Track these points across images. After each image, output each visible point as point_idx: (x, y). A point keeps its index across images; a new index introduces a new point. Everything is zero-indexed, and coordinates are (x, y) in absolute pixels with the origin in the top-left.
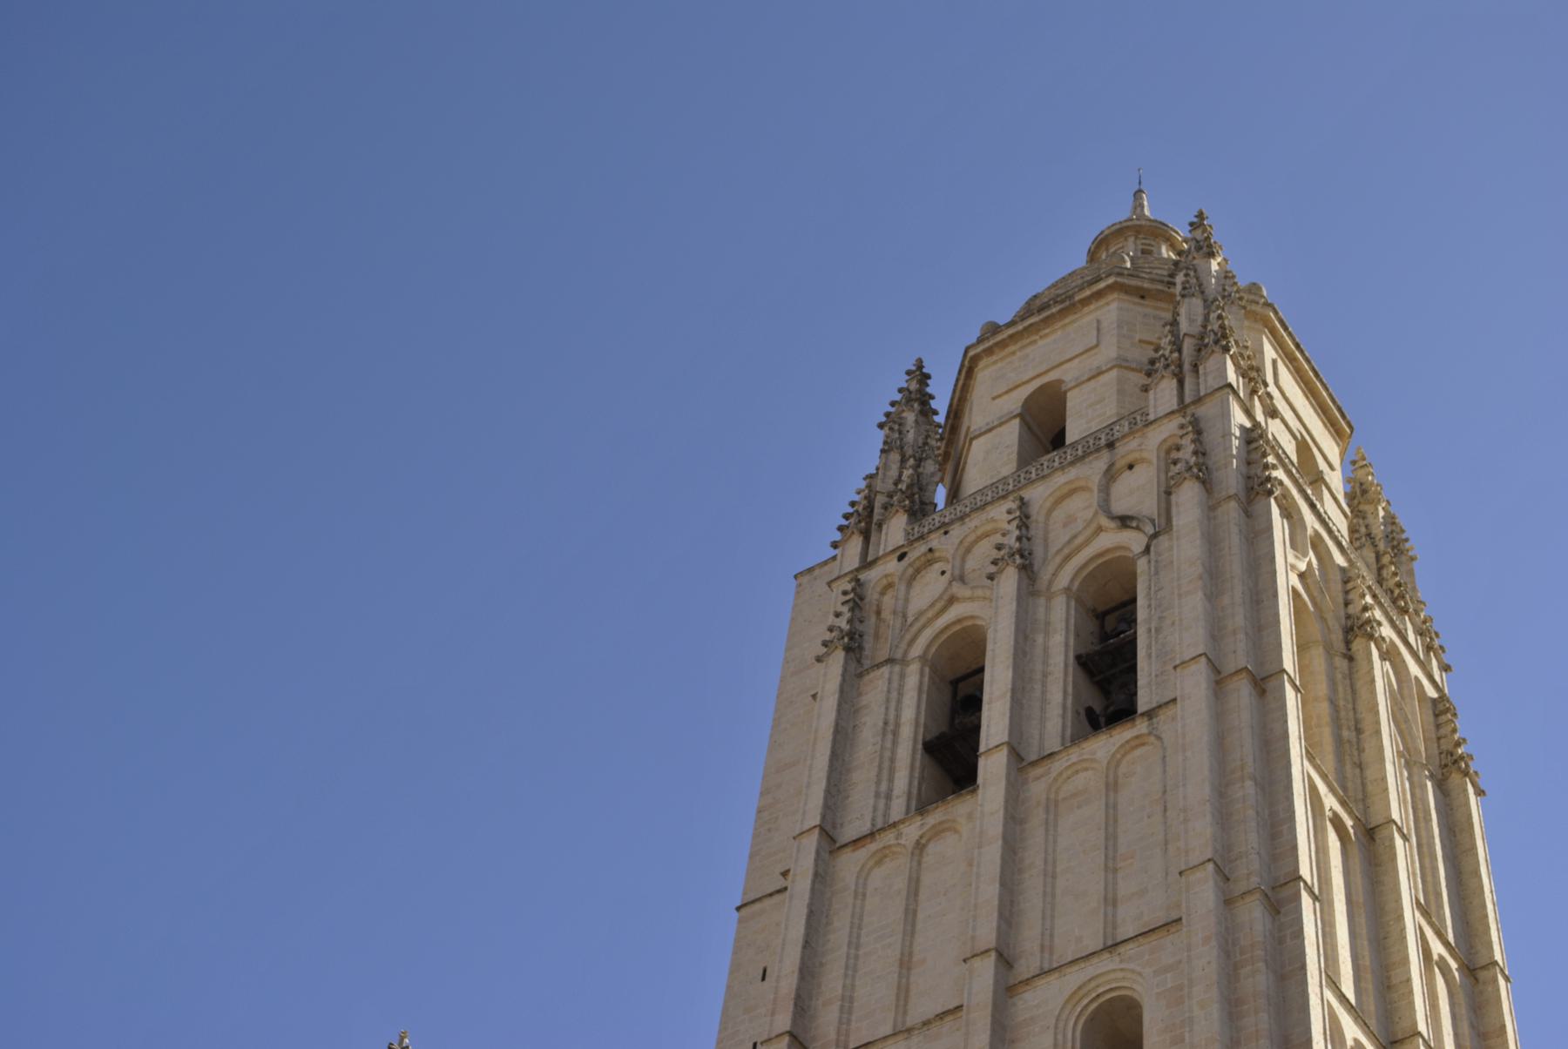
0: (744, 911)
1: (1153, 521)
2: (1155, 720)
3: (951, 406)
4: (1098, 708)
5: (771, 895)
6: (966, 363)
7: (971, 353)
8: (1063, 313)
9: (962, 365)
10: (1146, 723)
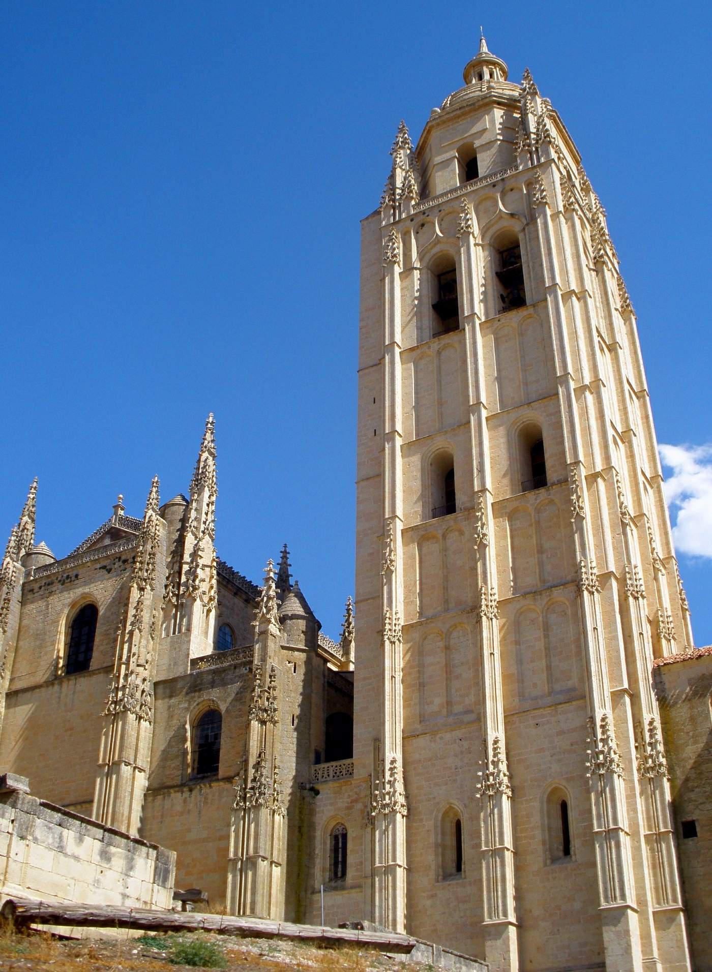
0: (361, 373)
1: (525, 217)
3: (419, 144)
4: (505, 295)
6: (428, 128)
7: (430, 124)
8: (470, 111)
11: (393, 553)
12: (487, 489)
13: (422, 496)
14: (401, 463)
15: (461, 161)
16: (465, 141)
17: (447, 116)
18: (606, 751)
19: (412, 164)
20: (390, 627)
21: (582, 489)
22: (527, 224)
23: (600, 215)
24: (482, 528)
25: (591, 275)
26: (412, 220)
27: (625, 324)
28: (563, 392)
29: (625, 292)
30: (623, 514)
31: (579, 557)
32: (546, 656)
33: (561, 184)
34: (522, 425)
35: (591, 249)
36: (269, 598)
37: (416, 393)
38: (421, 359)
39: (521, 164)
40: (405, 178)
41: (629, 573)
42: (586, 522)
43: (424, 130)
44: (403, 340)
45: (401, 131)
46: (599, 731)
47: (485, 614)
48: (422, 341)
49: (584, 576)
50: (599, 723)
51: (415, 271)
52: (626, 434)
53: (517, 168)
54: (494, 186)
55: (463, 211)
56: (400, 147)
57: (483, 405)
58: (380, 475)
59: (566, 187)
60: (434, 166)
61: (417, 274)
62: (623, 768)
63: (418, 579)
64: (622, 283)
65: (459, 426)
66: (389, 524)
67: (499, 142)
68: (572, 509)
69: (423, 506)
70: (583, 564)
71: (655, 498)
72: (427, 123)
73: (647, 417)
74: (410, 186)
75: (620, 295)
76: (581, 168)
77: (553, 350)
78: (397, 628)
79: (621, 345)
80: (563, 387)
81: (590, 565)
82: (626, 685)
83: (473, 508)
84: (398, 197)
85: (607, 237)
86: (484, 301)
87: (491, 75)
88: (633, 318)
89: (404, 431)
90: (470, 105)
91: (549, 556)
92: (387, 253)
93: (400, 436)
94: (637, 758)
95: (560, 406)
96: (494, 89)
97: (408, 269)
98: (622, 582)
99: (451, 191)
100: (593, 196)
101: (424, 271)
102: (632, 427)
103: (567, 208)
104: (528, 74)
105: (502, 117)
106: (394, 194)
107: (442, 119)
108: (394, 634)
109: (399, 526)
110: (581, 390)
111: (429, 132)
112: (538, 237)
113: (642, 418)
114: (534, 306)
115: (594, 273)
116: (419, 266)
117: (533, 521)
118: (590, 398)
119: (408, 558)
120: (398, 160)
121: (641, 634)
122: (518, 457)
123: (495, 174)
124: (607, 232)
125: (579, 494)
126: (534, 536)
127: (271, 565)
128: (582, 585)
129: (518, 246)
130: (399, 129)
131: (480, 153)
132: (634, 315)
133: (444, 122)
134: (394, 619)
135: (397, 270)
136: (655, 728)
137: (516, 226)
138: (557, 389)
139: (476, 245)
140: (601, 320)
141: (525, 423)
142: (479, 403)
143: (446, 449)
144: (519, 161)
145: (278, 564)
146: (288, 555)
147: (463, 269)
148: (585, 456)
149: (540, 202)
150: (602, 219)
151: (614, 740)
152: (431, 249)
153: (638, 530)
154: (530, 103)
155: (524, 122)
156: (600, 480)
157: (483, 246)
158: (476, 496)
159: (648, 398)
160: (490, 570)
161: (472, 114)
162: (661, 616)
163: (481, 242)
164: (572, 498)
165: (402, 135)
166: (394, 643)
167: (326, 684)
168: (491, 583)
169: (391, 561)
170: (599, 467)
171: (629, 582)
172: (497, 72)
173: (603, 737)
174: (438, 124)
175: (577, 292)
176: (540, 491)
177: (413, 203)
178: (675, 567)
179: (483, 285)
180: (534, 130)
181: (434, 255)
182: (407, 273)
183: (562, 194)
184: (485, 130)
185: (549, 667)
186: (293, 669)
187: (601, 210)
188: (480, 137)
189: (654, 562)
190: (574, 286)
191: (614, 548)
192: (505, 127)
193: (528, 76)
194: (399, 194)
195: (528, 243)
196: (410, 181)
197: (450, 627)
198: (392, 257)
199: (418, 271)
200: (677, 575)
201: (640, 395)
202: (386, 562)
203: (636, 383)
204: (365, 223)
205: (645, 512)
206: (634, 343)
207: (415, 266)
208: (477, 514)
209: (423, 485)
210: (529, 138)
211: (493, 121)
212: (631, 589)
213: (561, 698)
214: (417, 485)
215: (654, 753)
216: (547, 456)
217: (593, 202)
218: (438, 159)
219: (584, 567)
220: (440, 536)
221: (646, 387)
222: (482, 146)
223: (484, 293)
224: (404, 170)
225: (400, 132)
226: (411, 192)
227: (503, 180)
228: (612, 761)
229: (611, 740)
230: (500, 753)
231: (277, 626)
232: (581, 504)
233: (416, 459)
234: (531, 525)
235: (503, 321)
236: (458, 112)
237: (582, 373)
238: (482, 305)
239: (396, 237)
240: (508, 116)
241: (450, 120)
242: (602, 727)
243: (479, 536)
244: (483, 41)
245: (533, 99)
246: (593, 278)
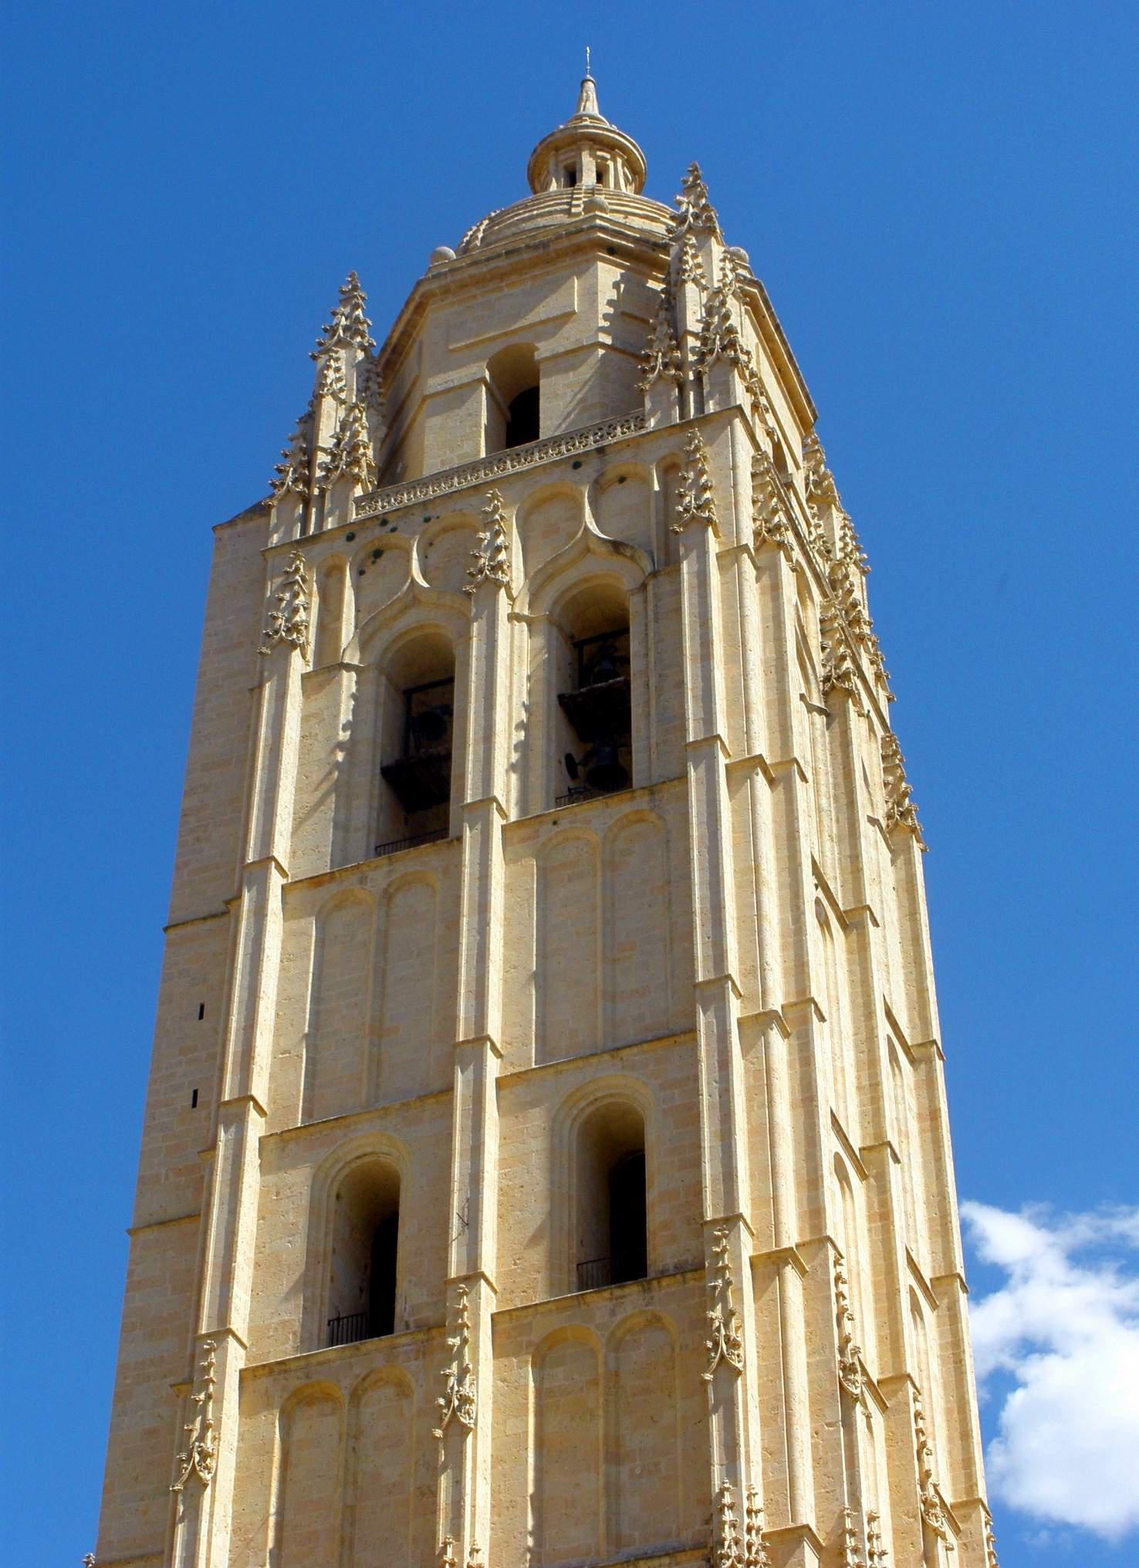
0: (172, 933)
1: (651, 553)
2: (657, 796)
3: (390, 338)
5: (205, 919)
6: (417, 297)
7: (422, 289)
8: (533, 264)
10: (647, 798)
11: (210, 1434)
12: (483, 1276)
13: (305, 1283)
14: (257, 1187)
15: (496, 392)
16: (515, 340)
17: (473, 271)
19: (367, 389)
21: (740, 1290)
22: (654, 574)
23: (852, 569)
24: (460, 1382)
25: (813, 724)
26: (351, 538)
27: (893, 862)
28: (708, 1025)
29: (901, 779)
30: (848, 1369)
33: (754, 475)
34: (591, 1109)
35: (818, 656)
37: (316, 999)
38: (338, 907)
39: (653, 413)
40: (344, 426)
41: (853, 1534)
42: (745, 1385)
43: (407, 304)
44: (294, 853)
45: (347, 298)
48: (345, 860)
49: (728, 1533)
51: (345, 674)
52: (874, 1154)
53: (641, 421)
54: (577, 465)
55: (489, 523)
56: (340, 343)
57: (493, 1044)
58: (198, 1216)
59: (767, 484)
60: (424, 399)
61: (348, 682)
63: (273, 1510)
64: (895, 753)
65: (421, 1098)
66: (208, 1351)
67: (601, 352)
68: (710, 1344)
69: (305, 1308)
70: (727, 1499)
71: (941, 1335)
72: (419, 283)
73: (934, 1115)
74: (355, 447)
75: (886, 784)
76: (815, 442)
77: (690, 912)
79: (879, 919)
80: (711, 1013)
81: (746, 1504)
83: (442, 1325)
84: (319, 473)
85: (866, 630)
86: (521, 767)
87: (601, 177)
88: (917, 848)
89: (273, 1100)
90: (536, 247)
91: (638, 1471)
92: (275, 618)
93: (261, 1111)
95: (696, 1062)
96: (603, 209)
97: (327, 668)
99: (461, 471)
100: (837, 518)
101: (371, 675)
102: (892, 1136)
103: (764, 541)
104: (697, 178)
105: (616, 285)
106: (309, 464)
107: (458, 276)
109: (236, 1359)
110: (760, 1023)
111: (420, 308)
112: (678, 610)
113: (920, 1117)
114: (651, 790)
115: (820, 720)
116: (356, 662)
117: (601, 1370)
118: (780, 1047)
119: (251, 1451)
120: (331, 375)
122: (574, 1193)
123: (583, 435)
124: (865, 614)
125: (731, 1306)
126: (601, 1413)
128: (722, 1557)
129: (627, 630)
130: (343, 293)
131: (549, 375)
132: (918, 841)
133: (463, 286)
135: (299, 665)
137: (622, 576)
138: (693, 1016)
139: (513, 617)
140: (828, 845)
141: (599, 1104)
142: (481, 1038)
143: (382, 1159)
144: (648, 405)
147: (473, 677)
148: (756, 1202)
149: (693, 517)
150: (856, 578)
152: (395, 618)
153: (886, 1420)
154: (694, 256)
155: (672, 303)
156: (790, 1273)
157: (530, 622)
158: (450, 1294)
159: (939, 1064)
160: (474, 1499)
161: (537, 272)
163: (526, 612)
165: (347, 310)
168: (473, 1536)
169: (205, 1455)
170: (792, 1234)
172: (617, 169)
174: (446, 291)
175: (768, 762)
176: (627, 1291)
177: (358, 491)
178: (986, 1532)
179: (521, 726)
180: (697, 328)
181: (401, 635)
182: (321, 678)
183: (754, 502)
184: (568, 316)
187: (857, 555)
188: (553, 334)
189: (927, 1512)
190: (762, 746)
191: (817, 1461)
192: (623, 314)
193: (694, 185)
195: (651, 625)
196: (355, 434)
198: (289, 631)
199: (354, 674)
201: (919, 1055)
202: (190, 1457)
203: (911, 1020)
204: (226, 533)
205: (911, 1368)
206: (913, 914)
207: (346, 660)
208: (451, 1341)
209: (311, 1253)
210: (680, 345)
211: (590, 294)
214: (295, 1250)
216: (652, 1195)
217: (838, 533)
218: (435, 383)
219: (731, 1507)
220: (344, 1394)
221: (936, 1034)
222: (555, 357)
223: (523, 747)
224: (343, 402)
225: (344, 302)
226: (356, 462)
227: (601, 451)
232: (733, 1334)
233: (299, 1179)
234: (595, 1382)
235: (564, 824)
236: (502, 263)
237: (763, 978)
238: (514, 777)
239: (304, 580)
240: (632, 284)
241: (479, 281)
243: (449, 1402)
244: (590, 86)
245: (702, 246)
246: (818, 733)
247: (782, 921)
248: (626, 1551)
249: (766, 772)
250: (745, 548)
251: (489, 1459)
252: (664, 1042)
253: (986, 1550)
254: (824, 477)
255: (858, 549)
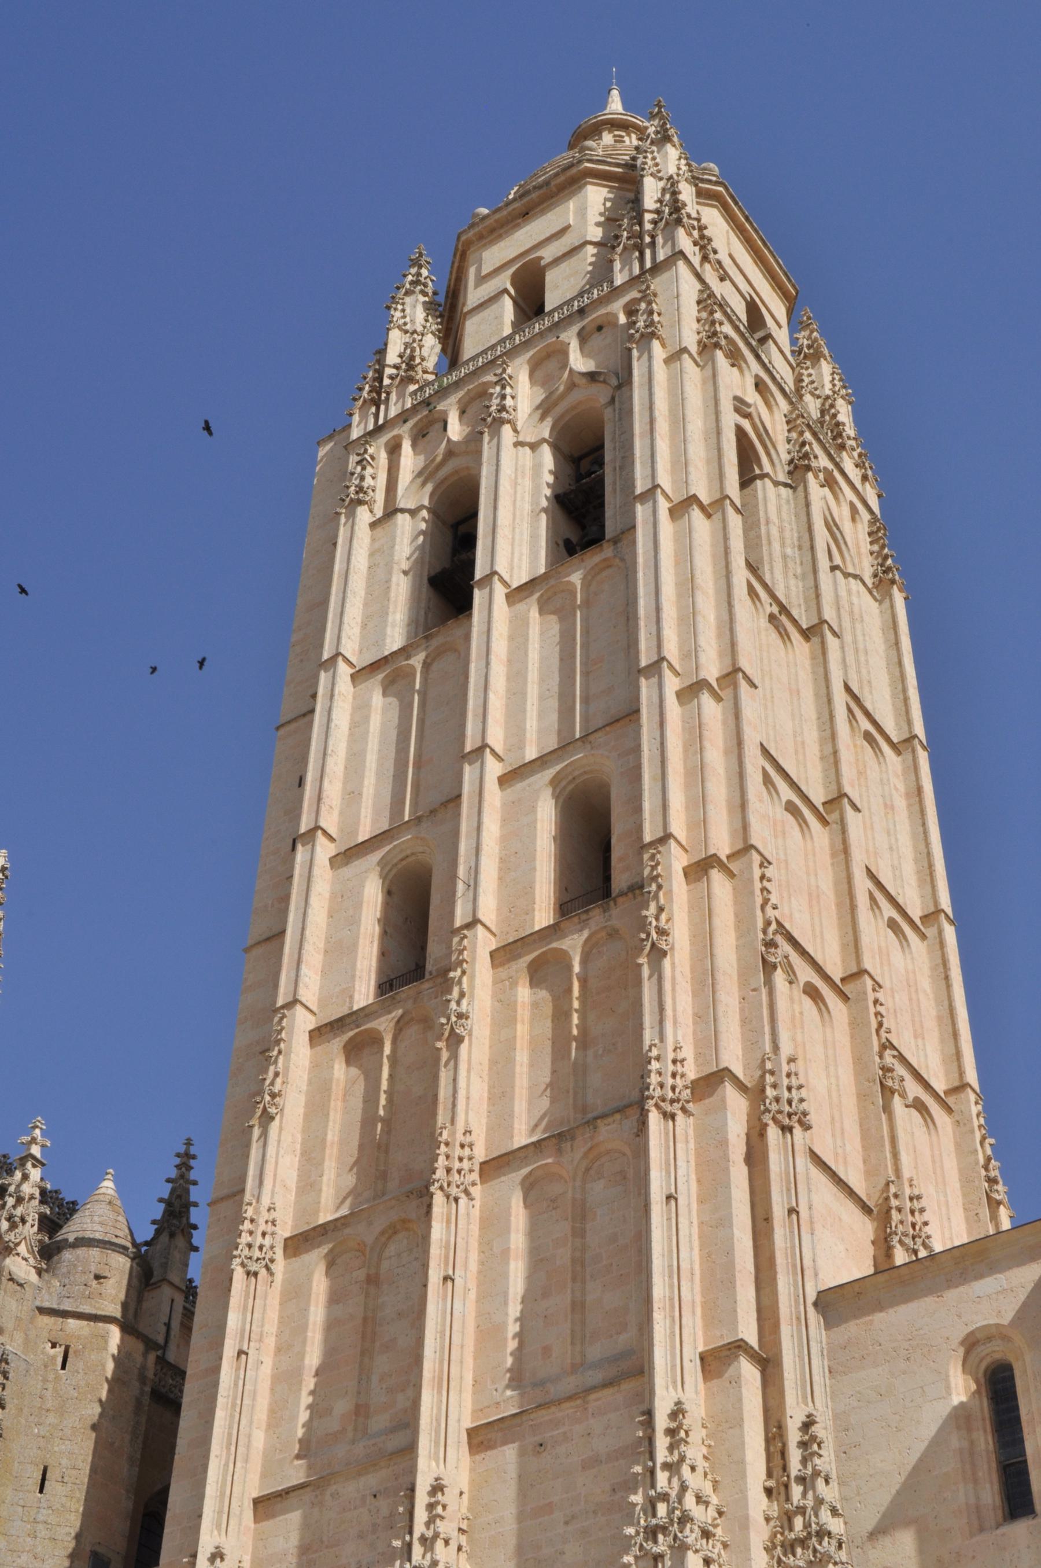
0: (281, 732)
2: (619, 545)
3: (449, 286)
4: (574, 539)
6: (460, 247)
7: (464, 238)
9: (456, 249)
11: (279, 1081)
17: (497, 216)
18: (673, 1494)
20: (249, 1239)
24: (458, 1003)
29: (883, 547)
31: (648, 1036)
32: (574, 1279)
34: (571, 787)
35: (783, 448)
36: (20, 1200)
40: (407, 345)
41: (772, 1073)
42: (673, 964)
43: (455, 255)
46: (662, 1442)
47: (441, 1188)
50: (661, 1421)
62: (725, 1546)
64: (879, 529)
70: (655, 1052)
76: (809, 318)
78: (267, 1241)
79: (836, 628)
82: (752, 1338)
89: (341, 830)
91: (600, 1052)
94: (768, 1519)
98: (756, 1094)
100: (826, 368)
102: (848, 789)
103: (705, 346)
107: (487, 222)
108: (257, 1254)
113: (908, 795)
121: (792, 1211)
125: (662, 901)
127: (37, 1132)
128: (648, 1098)
130: (412, 260)
132: (900, 590)
133: (492, 231)
134: (262, 1221)
135: (364, 516)
136: (814, 1438)
141: (578, 781)
145: (168, 1181)
146: (192, 1162)
151: (701, 1465)
153: (849, 1009)
159: (923, 757)
162: (896, 1196)
164: (644, 913)
166: (256, 1274)
167: (146, 1400)
170: (722, 844)
171: (770, 1092)
173: (669, 1460)
174: (481, 237)
177: (413, 388)
178: (975, 1110)
185: (578, 1307)
186: (60, 1360)
187: (843, 392)
189: (885, 1076)
191: (744, 1022)
194: (391, 377)
196: (413, 350)
197: (382, 1233)
200: (980, 1126)
207: (402, 505)
211: (582, 212)
212: (774, 1107)
213: (596, 1377)
215: (810, 1502)
217: (827, 379)
219: (658, 1058)
221: (919, 729)
228: (685, 1519)
229: (693, 1469)
230: (442, 1518)
231: (32, 1261)
239: (372, 458)
242: (671, 1432)
243: (449, 1019)
247: (718, 618)
248: (590, 1116)
249: (702, 507)
250: (685, 350)
251: (486, 1062)
252: (622, 722)
253: (976, 1123)
254: (816, 340)
255: (844, 387)
